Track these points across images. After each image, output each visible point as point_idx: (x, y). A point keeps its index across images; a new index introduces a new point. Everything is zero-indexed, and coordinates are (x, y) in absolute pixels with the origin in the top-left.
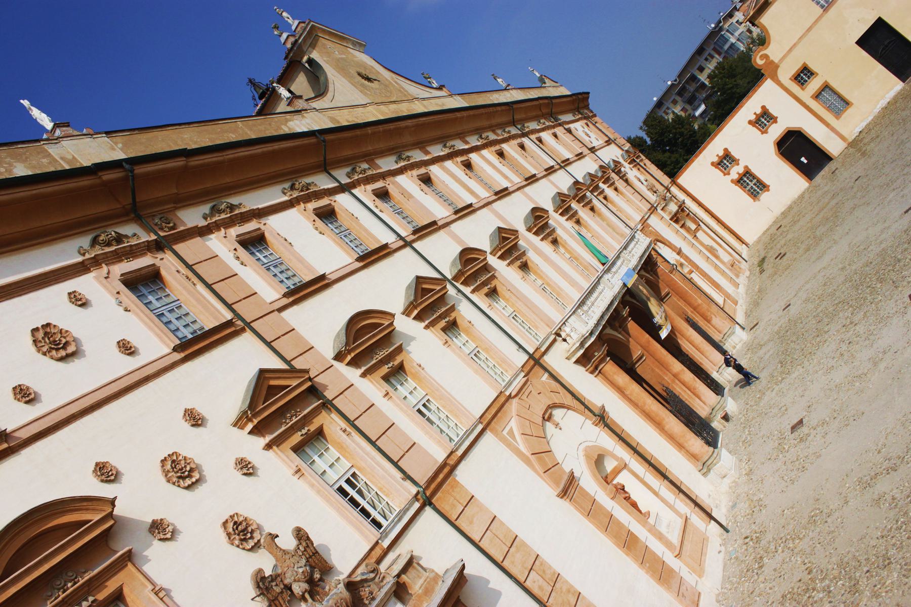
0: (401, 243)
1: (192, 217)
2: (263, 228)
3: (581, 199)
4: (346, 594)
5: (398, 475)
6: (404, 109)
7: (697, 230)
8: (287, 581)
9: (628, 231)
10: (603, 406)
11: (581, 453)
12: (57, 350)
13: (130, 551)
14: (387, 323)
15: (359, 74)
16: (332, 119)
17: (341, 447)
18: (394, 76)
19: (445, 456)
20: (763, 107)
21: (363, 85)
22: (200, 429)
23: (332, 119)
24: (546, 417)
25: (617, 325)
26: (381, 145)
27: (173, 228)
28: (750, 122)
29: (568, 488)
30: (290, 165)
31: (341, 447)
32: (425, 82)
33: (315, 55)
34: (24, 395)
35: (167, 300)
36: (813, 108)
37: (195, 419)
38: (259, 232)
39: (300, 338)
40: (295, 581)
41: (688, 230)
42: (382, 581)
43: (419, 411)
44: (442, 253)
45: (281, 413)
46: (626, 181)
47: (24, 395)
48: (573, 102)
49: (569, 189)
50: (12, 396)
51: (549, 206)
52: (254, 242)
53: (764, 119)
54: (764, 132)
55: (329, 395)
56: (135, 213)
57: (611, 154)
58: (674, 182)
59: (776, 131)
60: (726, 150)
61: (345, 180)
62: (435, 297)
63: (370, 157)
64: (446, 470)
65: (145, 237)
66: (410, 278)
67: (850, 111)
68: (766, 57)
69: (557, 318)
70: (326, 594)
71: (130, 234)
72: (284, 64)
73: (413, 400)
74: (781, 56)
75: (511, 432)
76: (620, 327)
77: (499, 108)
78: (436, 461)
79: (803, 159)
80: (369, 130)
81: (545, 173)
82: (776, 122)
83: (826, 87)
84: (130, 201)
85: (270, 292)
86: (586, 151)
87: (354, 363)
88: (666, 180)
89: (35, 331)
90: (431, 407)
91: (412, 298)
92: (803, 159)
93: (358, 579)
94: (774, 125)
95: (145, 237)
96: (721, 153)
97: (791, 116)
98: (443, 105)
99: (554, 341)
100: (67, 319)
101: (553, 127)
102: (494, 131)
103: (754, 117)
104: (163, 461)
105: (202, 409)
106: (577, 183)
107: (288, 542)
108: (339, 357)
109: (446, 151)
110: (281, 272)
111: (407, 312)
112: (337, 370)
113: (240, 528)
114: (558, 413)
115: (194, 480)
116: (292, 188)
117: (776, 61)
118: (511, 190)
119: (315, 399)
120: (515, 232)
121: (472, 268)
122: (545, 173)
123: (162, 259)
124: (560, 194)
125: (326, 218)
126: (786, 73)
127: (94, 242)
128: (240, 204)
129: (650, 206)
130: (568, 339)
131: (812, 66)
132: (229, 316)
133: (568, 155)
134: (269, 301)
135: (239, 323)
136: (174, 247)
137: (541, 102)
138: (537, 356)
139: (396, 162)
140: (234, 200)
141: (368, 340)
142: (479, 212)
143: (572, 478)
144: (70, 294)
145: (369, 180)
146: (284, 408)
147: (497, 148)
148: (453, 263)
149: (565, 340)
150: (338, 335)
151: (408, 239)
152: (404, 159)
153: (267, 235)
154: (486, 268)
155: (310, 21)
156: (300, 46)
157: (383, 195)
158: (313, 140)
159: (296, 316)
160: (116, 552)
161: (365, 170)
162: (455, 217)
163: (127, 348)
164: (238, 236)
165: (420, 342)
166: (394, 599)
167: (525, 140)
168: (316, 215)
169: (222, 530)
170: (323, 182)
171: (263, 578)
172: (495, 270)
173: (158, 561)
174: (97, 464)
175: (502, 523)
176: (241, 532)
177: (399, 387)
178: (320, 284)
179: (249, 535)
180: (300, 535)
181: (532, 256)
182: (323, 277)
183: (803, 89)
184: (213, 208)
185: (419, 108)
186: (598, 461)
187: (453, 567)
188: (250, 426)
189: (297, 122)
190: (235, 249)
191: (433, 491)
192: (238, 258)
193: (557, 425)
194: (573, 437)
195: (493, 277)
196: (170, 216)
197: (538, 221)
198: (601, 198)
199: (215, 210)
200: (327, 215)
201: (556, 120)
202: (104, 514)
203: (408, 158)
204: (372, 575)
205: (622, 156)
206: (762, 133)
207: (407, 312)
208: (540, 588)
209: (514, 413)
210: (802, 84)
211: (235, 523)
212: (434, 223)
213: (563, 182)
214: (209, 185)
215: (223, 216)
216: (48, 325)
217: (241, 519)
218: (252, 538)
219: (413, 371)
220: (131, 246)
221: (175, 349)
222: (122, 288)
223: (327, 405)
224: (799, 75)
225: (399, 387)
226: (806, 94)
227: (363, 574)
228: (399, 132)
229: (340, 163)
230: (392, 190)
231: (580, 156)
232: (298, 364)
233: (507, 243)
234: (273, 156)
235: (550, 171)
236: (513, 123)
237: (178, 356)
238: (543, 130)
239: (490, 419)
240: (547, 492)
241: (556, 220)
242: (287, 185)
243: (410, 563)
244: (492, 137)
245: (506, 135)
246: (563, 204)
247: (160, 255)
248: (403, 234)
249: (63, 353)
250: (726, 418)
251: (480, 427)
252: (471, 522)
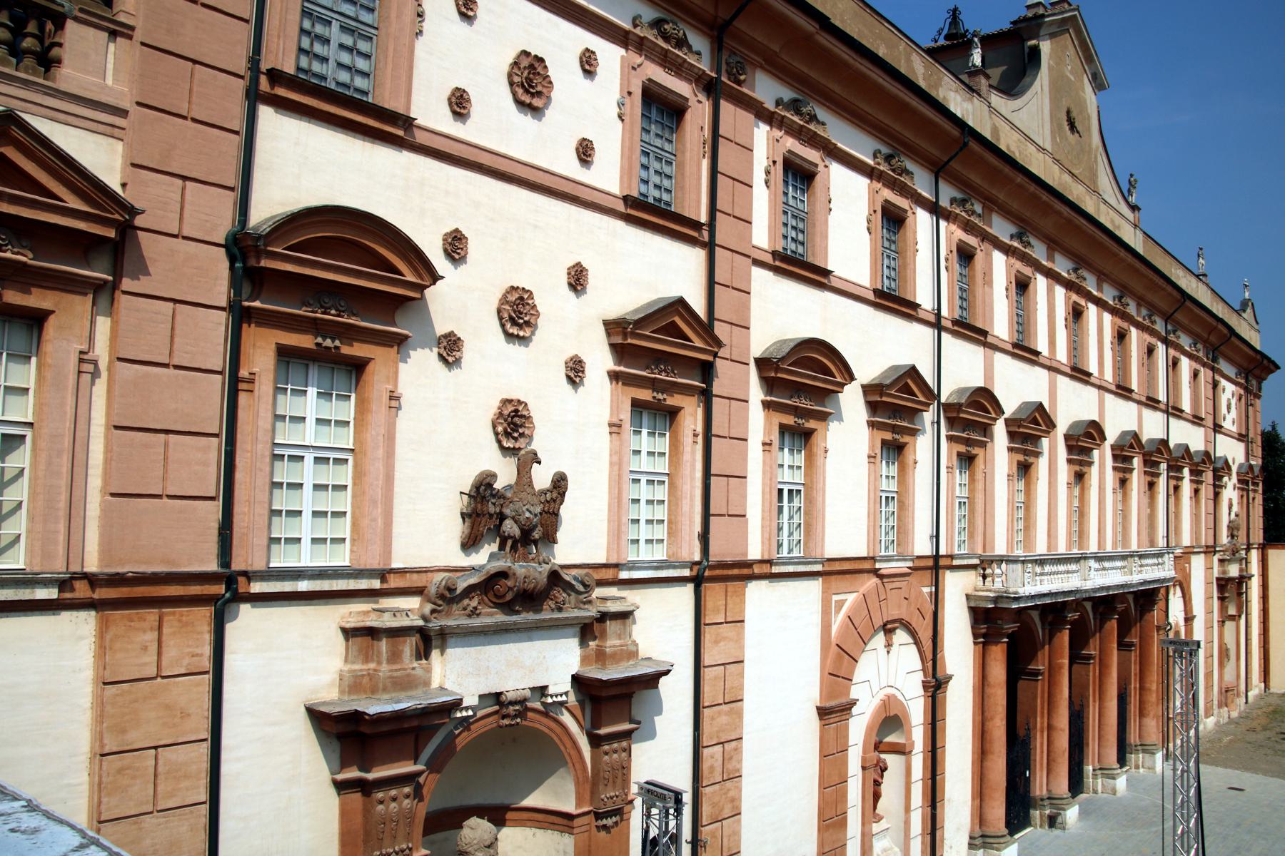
0: (932, 319)
1: (766, 89)
2: (821, 168)
3: (1150, 463)
4: (543, 579)
5: (698, 528)
6: (1076, 192)
7: (1232, 618)
8: (507, 511)
9: (1161, 543)
10: (950, 677)
11: (881, 695)
12: (527, 91)
13: (407, 337)
14: (839, 379)
15: (1068, 112)
16: (995, 130)
17: (675, 446)
18: (1101, 149)
19: (759, 557)
21: (1060, 127)
22: (572, 295)
23: (995, 130)
24: (889, 626)
25: (1050, 618)
26: (1015, 205)
27: (739, 83)
29: (833, 713)
30: (909, 135)
31: (675, 446)
32: (1125, 187)
33: (1046, 47)
34: (459, 104)
35: (667, 147)
37: (577, 280)
38: (812, 168)
39: (746, 307)
40: (513, 518)
41: (1223, 609)
42: (585, 603)
43: (781, 491)
44: (961, 369)
45: (658, 358)
46: (1217, 495)
47: (459, 104)
48: (1251, 359)
49: (1151, 441)
50: (448, 93)
51: (1112, 435)
52: (799, 175)
55: (719, 386)
56: (719, 34)
57: (1231, 451)
58: (1263, 548)
61: (944, 203)
62: (909, 404)
63: (992, 204)
64: (745, 571)
65: (704, 65)
66: (905, 360)
69: (1000, 549)
70: (526, 559)
71: (694, 49)
72: (1006, 26)
73: (787, 475)
75: (840, 604)
76: (1050, 624)
77: (1169, 289)
78: (746, 554)
80: (1020, 179)
81: (1144, 399)
84: (727, 18)
85: (762, 236)
86: (1210, 424)
87: (770, 384)
88: (1258, 536)
89: (525, 53)
90: (796, 500)
91: (888, 382)
93: (567, 578)
95: (704, 65)
98: (1118, 228)
99: (974, 567)
100: (563, 71)
101: (1204, 365)
102: (1139, 305)
104: (513, 289)
105: (593, 281)
106: (1165, 442)
107: (541, 478)
108: (762, 363)
109: (1073, 277)
110: (794, 228)
111: (867, 389)
112: (748, 374)
113: (516, 419)
114: (901, 636)
115: (521, 333)
116: (888, 158)
118: (1092, 380)
119: (700, 378)
120: (1051, 425)
121: (972, 416)
122: (1144, 399)
123: (699, 102)
124: (1136, 436)
125: (889, 221)
127: (657, 24)
128: (823, 124)
129: (1211, 543)
130: (989, 579)
132: (704, 218)
133: (1186, 406)
134: (755, 242)
135: (706, 235)
136: (723, 104)
137: (1220, 326)
138: (942, 562)
139: (1012, 237)
140: (822, 114)
141: (805, 377)
142: (1037, 369)
143: (847, 708)
144: (587, 50)
145: (968, 227)
146: (663, 358)
147: (1125, 325)
148: (961, 391)
149: (984, 577)
150: (785, 341)
151: (944, 323)
152: (1022, 242)
153: (818, 178)
154: (986, 430)
155: (1077, 9)
156: (1040, 26)
157: (965, 255)
158: (955, 132)
159: (764, 283)
160: (394, 325)
161: (974, 212)
162: (1009, 348)
163: (585, 152)
164: (790, 151)
165: (849, 431)
166: (578, 629)
167: (1161, 348)
168: (883, 208)
169: (497, 404)
170: (922, 182)
171: (490, 486)
172: (992, 440)
173: (417, 371)
174: (457, 230)
175: (741, 675)
176: (512, 423)
177: (786, 450)
178: (817, 276)
179: (516, 435)
180: (560, 483)
181: (1042, 464)
182: (826, 273)
184: (795, 101)
185: (1089, 205)
186: (890, 720)
187: (658, 662)
188: (618, 340)
189: (959, 98)
190: (774, 162)
191: (715, 577)
192: (768, 172)
193: (889, 645)
194: (889, 672)
195: (983, 445)
196: (749, 70)
197: (1084, 439)
198: (1172, 483)
199: (795, 106)
200: (893, 220)
201: (1215, 360)
202: (419, 281)
203: (1028, 244)
204: (581, 588)
205: (1241, 466)
207: (867, 389)
209: (863, 590)
211: (516, 411)
212: (984, 333)
213: (1153, 426)
214: (814, 75)
215: (796, 119)
216: (541, 60)
217: (525, 413)
218: (516, 439)
219: (815, 450)
220: (685, 60)
221: (626, 199)
222: (638, 93)
223: (706, 396)
225: (786, 450)
227: (575, 578)
228: (1047, 210)
229: (958, 181)
230: (979, 258)
231: (1197, 420)
232: (720, 330)
233: (1030, 427)
234: (902, 110)
235: (1151, 403)
236: (1167, 318)
237: (621, 207)
238: (1190, 356)
239: (837, 572)
240: (809, 692)
241: (1103, 458)
242: (885, 150)
243: (625, 616)
244: (1132, 309)
245: (1147, 323)
246: (1128, 448)
247: (702, 97)
248: (945, 312)
249: (527, 99)
250: (1052, 821)
251: (818, 568)
252: (716, 642)
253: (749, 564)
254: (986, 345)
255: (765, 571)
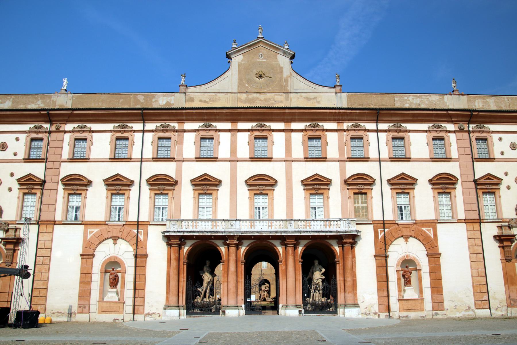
191: (46, 223)
208: (39, 261)
223: (42, 190)
253: (55, 221)
254: (175, 161)
255: (60, 223)
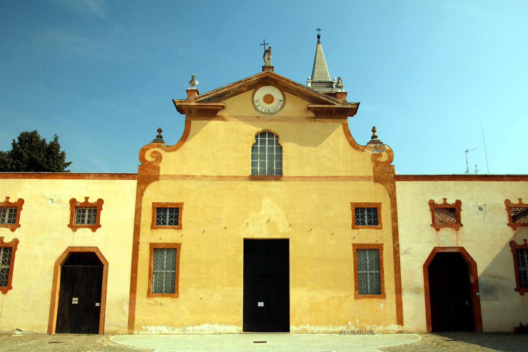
20: (100, 202)
28: (73, 202)
36: (140, 257)
53: (87, 214)
54: (73, 227)
59: (84, 239)
60: (21, 202)
67: (166, 300)
68: (159, 158)
74: (171, 172)
79: (75, 301)
82: (94, 230)
83: (174, 250)
92: (75, 301)
94: (89, 230)
96: (13, 200)
97: (113, 242)
103: (83, 200)
117: (162, 172)
126: (158, 193)
131: (185, 217)
183: (152, 227)
206: (70, 226)
210: (159, 223)
224: (165, 209)
226: (152, 236)
